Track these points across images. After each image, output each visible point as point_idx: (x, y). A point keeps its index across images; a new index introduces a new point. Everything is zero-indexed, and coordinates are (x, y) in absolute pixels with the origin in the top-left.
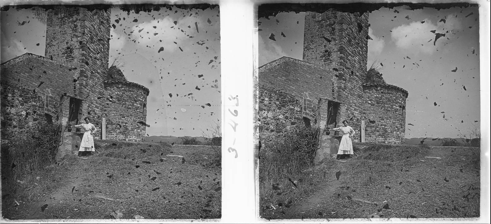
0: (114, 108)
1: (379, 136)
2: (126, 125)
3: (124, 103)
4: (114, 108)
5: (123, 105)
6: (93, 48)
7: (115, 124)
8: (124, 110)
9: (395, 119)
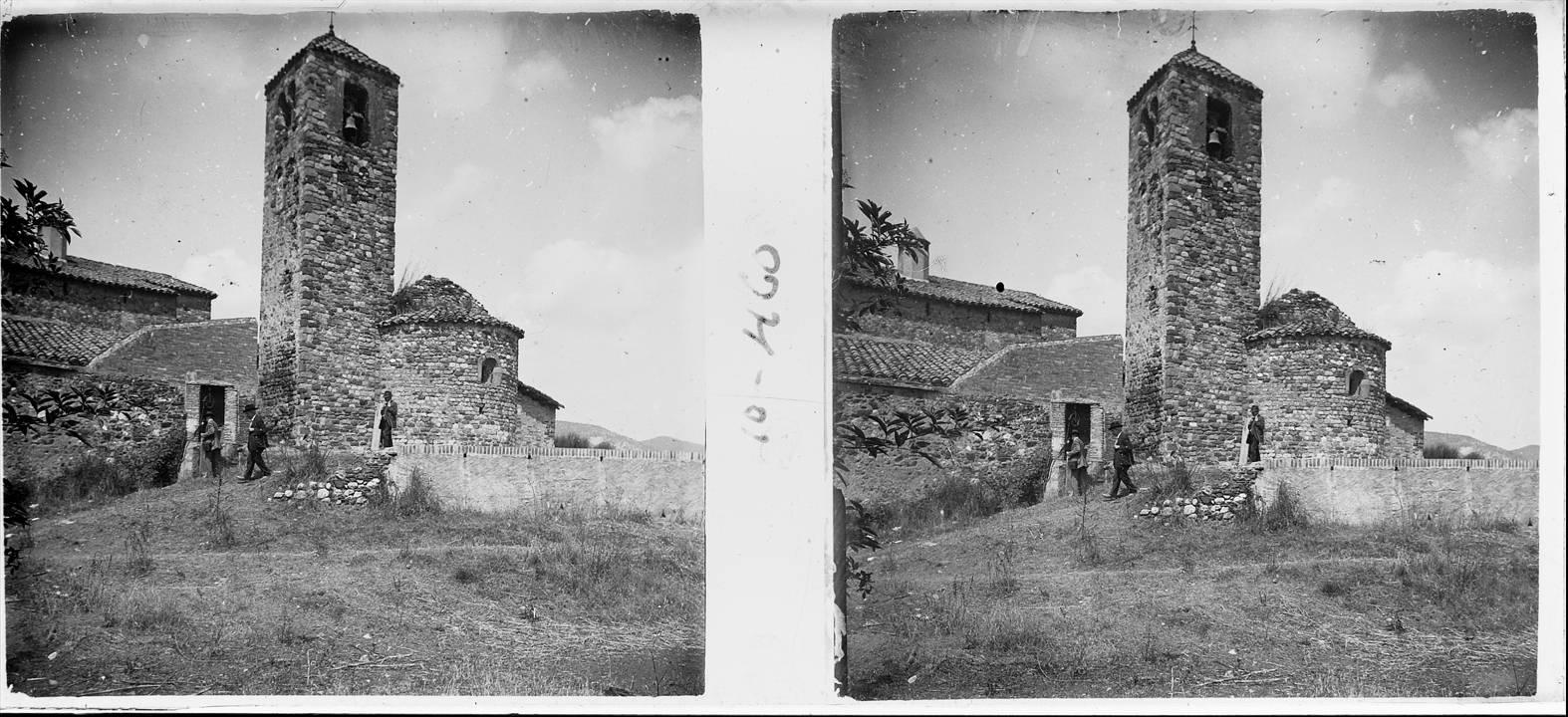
0: (1268, 393)
1: (1283, 451)
2: (1297, 429)
3: (1289, 378)
4: (1268, 393)
5: (1287, 383)
6: (334, 260)
7: (1270, 429)
8: (1290, 396)
9: (1322, 406)
